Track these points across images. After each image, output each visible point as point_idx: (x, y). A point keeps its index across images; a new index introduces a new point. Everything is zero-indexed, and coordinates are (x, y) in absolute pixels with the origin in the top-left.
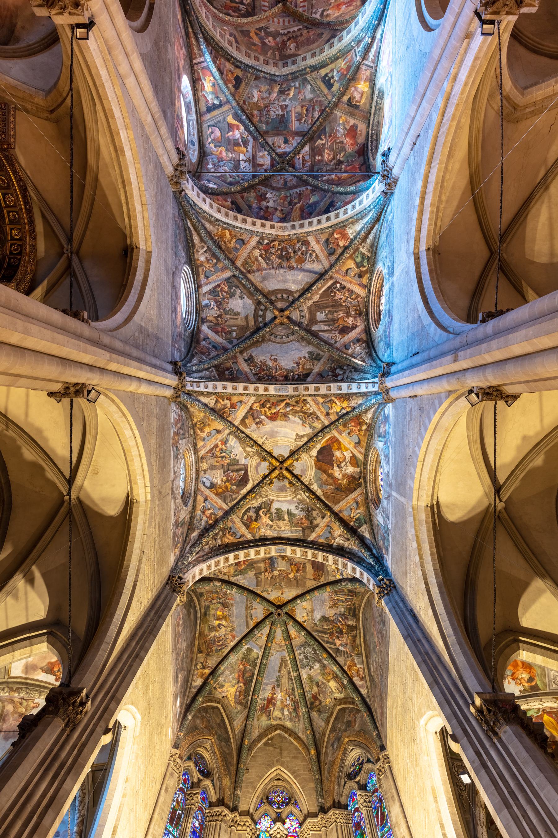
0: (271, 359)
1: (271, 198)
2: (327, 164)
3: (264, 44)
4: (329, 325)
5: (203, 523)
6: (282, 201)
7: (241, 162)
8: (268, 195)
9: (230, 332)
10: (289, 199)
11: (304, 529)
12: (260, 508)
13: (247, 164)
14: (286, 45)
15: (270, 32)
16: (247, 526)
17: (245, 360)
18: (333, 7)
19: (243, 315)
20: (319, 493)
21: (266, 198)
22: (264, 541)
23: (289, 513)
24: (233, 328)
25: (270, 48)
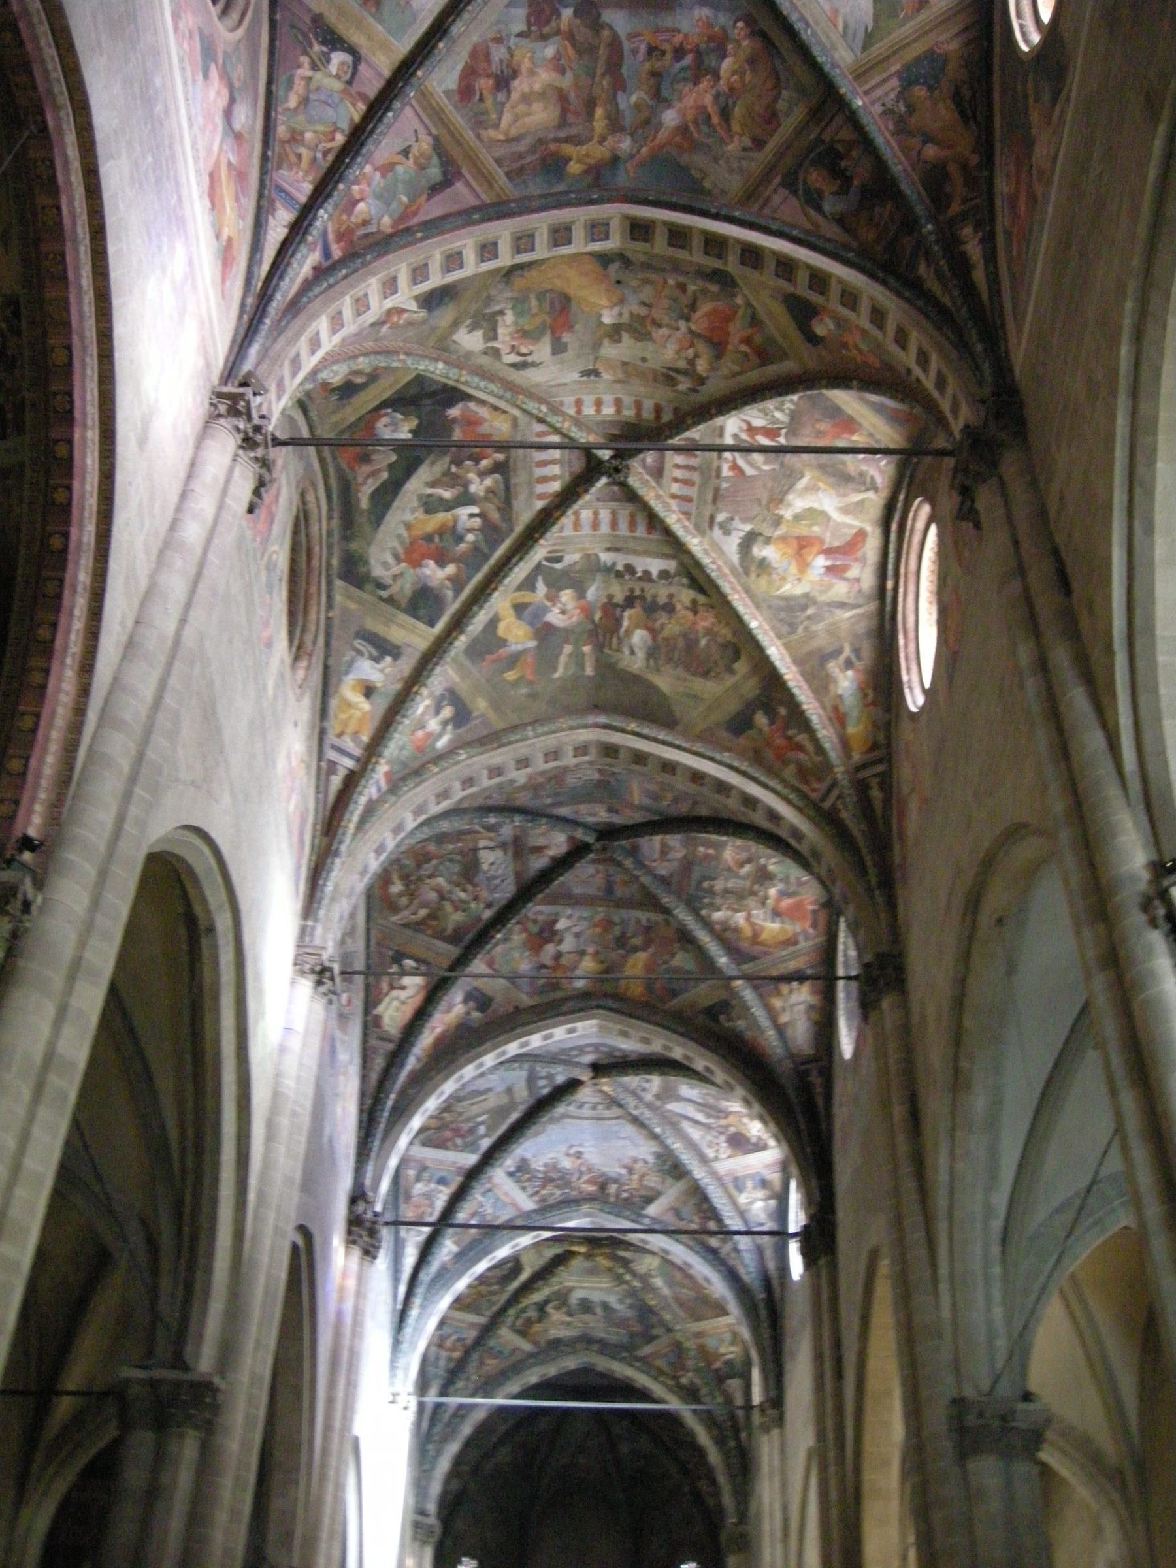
0: (568, 1155)
1: (568, 929)
2: (729, 869)
3: (545, 633)
4: (709, 1116)
5: (442, 1363)
6: (598, 930)
7: (482, 854)
8: (561, 925)
9: (472, 1131)
10: (617, 930)
11: (632, 1335)
12: (546, 1302)
13: (499, 854)
14: (618, 622)
15: (565, 573)
16: (523, 1333)
17: (511, 1174)
18: (783, 539)
19: (500, 1088)
20: (666, 1291)
21: (554, 933)
22: (556, 1346)
23: (605, 1306)
24: (480, 1119)
25: (566, 634)
